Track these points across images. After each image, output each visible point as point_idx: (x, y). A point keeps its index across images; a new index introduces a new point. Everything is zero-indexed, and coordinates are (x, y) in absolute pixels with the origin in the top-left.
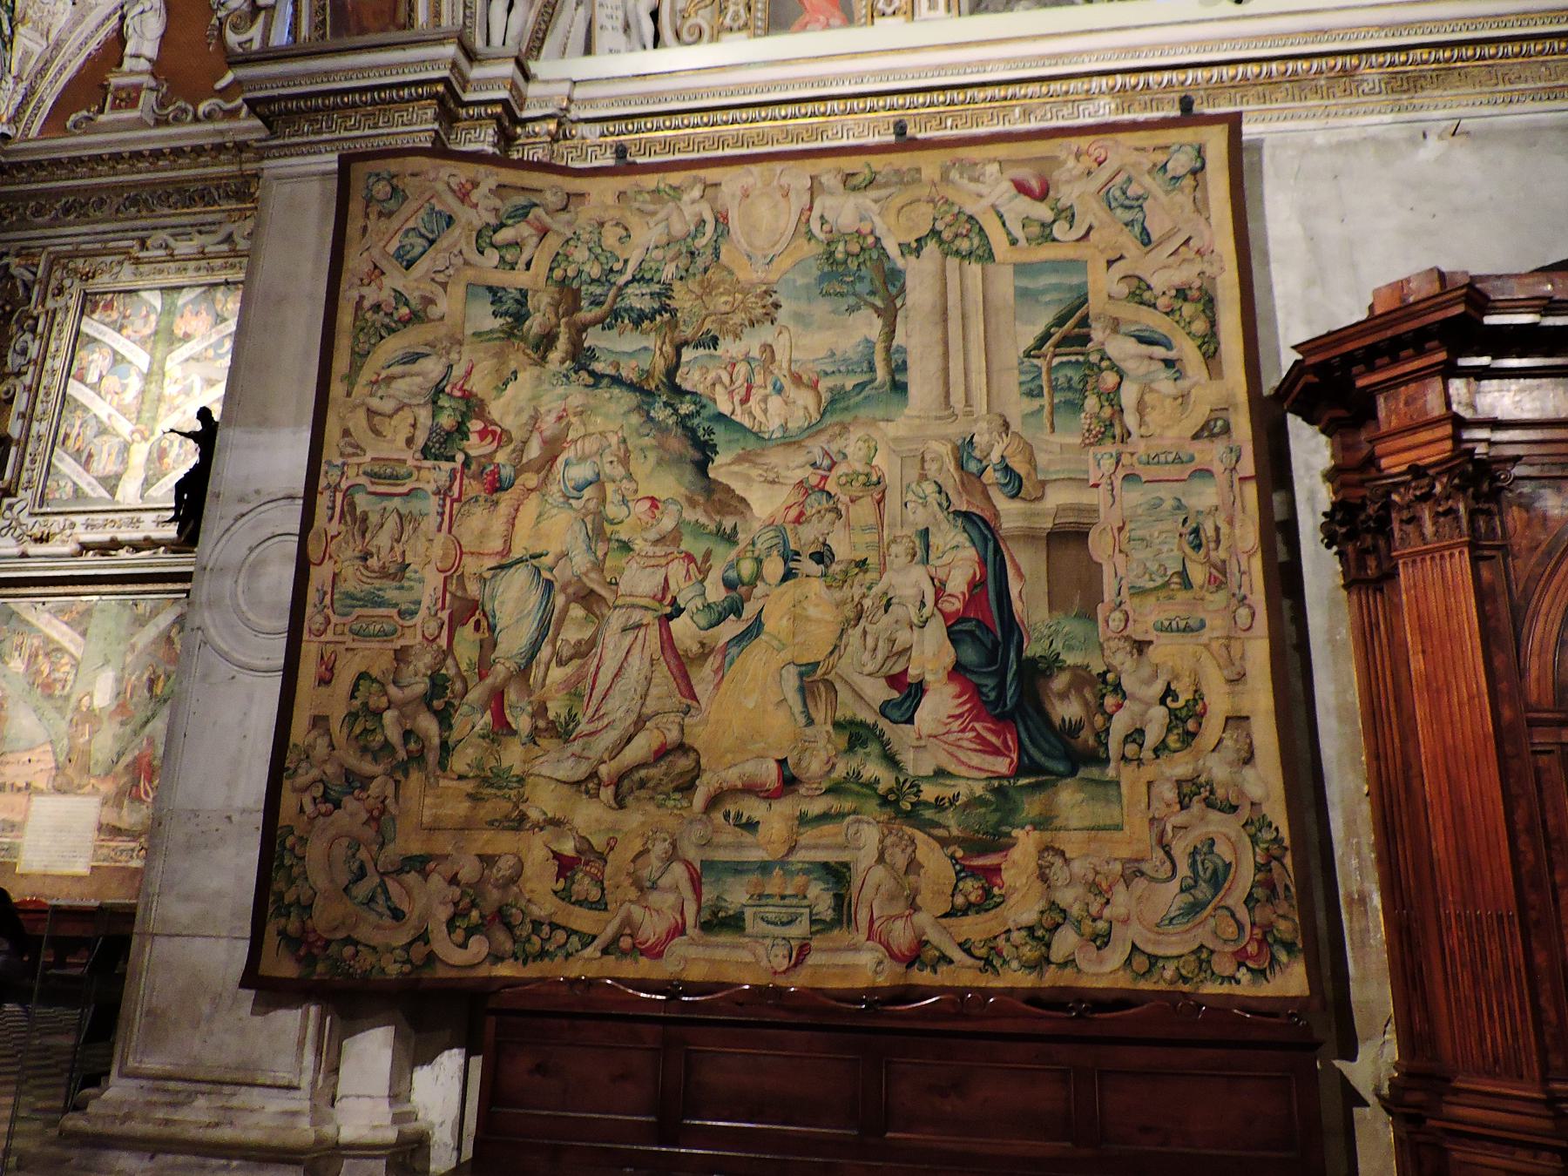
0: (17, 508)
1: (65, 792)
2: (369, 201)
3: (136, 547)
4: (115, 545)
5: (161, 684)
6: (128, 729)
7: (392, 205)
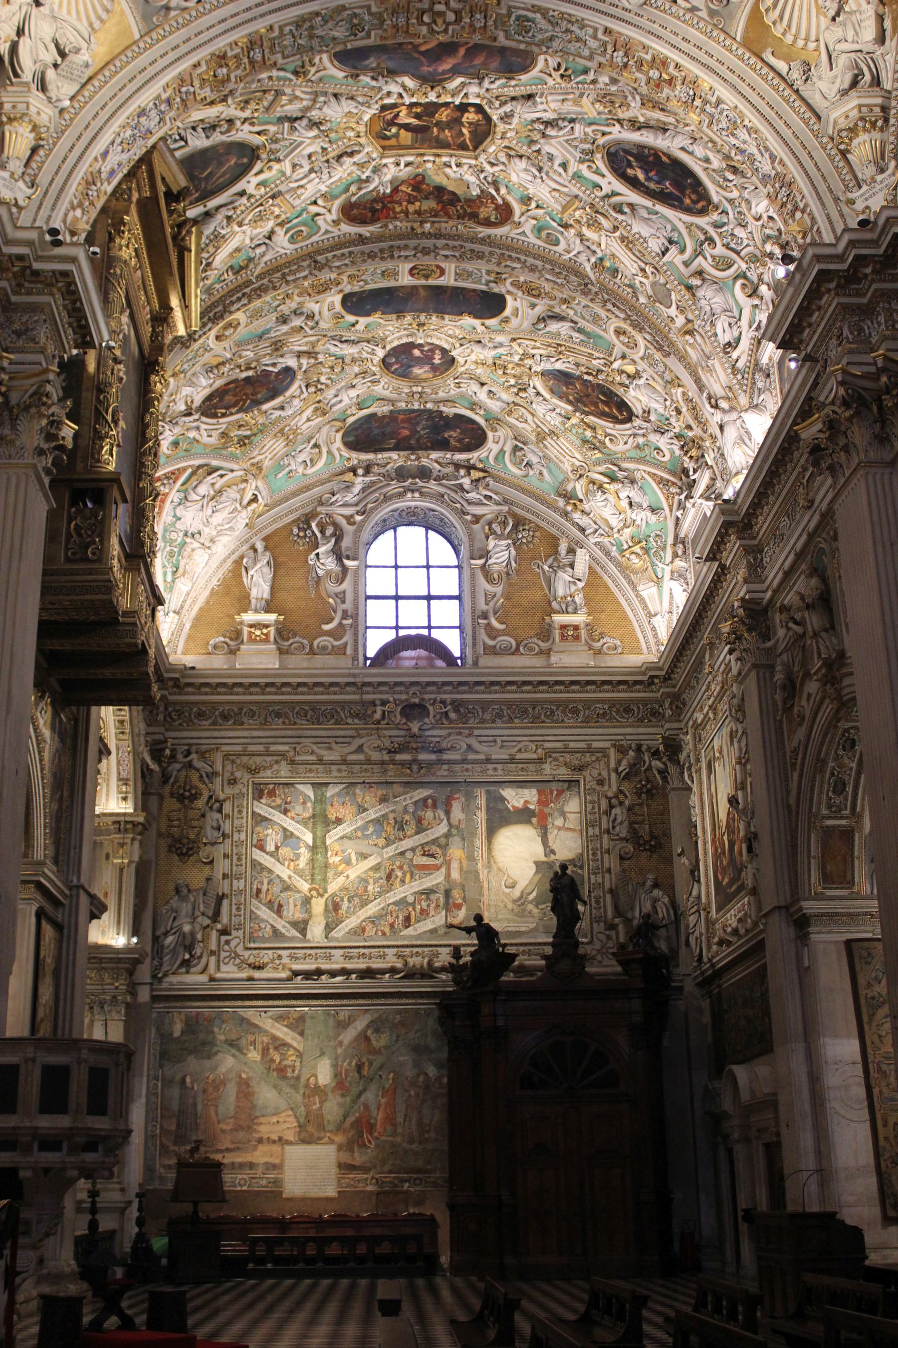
0: (233, 943)
1: (309, 1143)
2: (861, 957)
3: (333, 974)
4: (319, 972)
5: (366, 1068)
6: (348, 1099)
7: (869, 960)
